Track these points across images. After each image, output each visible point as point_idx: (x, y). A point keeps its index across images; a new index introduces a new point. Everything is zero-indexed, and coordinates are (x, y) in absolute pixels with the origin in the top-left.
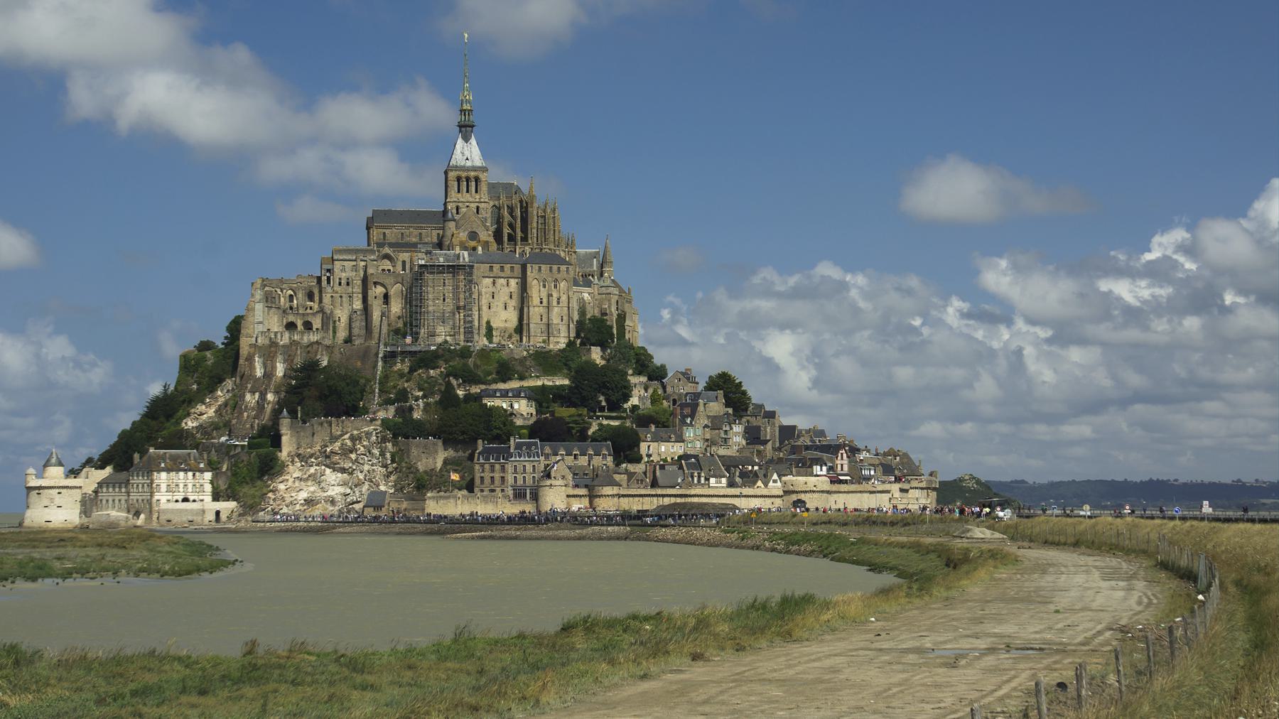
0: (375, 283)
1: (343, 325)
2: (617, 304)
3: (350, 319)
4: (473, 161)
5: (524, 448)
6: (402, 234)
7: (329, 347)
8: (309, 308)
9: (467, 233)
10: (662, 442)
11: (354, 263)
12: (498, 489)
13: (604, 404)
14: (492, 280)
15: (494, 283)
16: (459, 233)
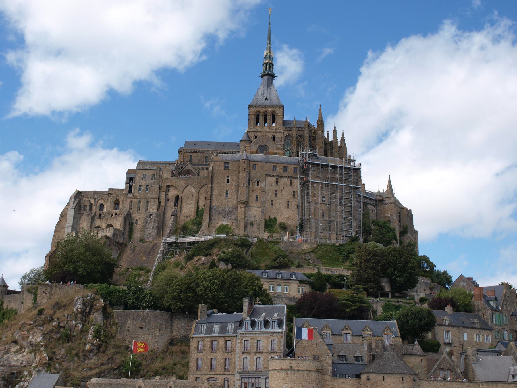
0: (168, 186)
1: (139, 227)
2: (399, 216)
3: (146, 222)
4: (271, 100)
5: (263, 315)
6: (206, 157)
7: (121, 244)
8: (114, 214)
9: (257, 146)
10: (464, 327)
11: (154, 172)
12: (221, 378)
13: (387, 288)
14: (275, 179)
15: (277, 182)
16: (250, 146)
